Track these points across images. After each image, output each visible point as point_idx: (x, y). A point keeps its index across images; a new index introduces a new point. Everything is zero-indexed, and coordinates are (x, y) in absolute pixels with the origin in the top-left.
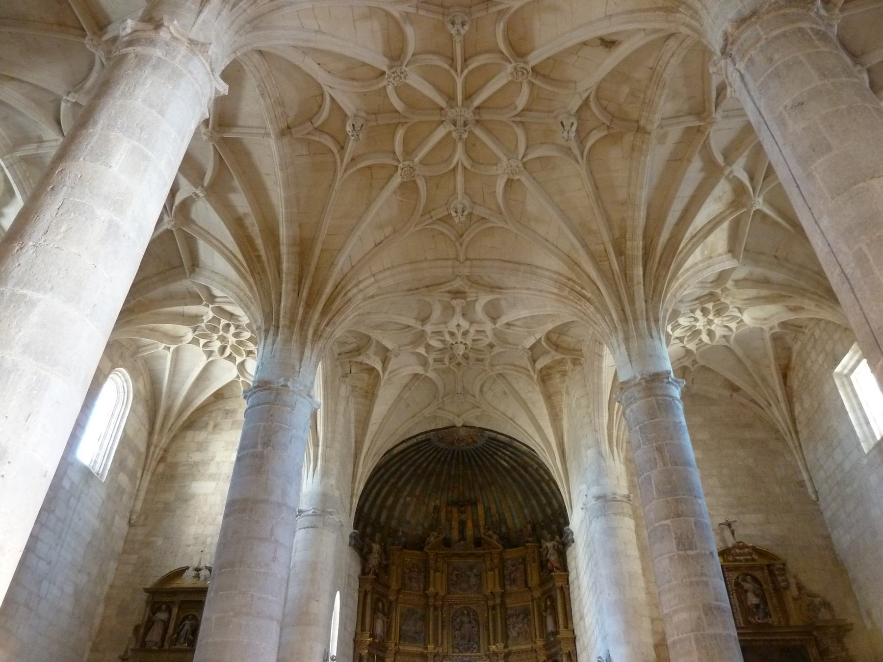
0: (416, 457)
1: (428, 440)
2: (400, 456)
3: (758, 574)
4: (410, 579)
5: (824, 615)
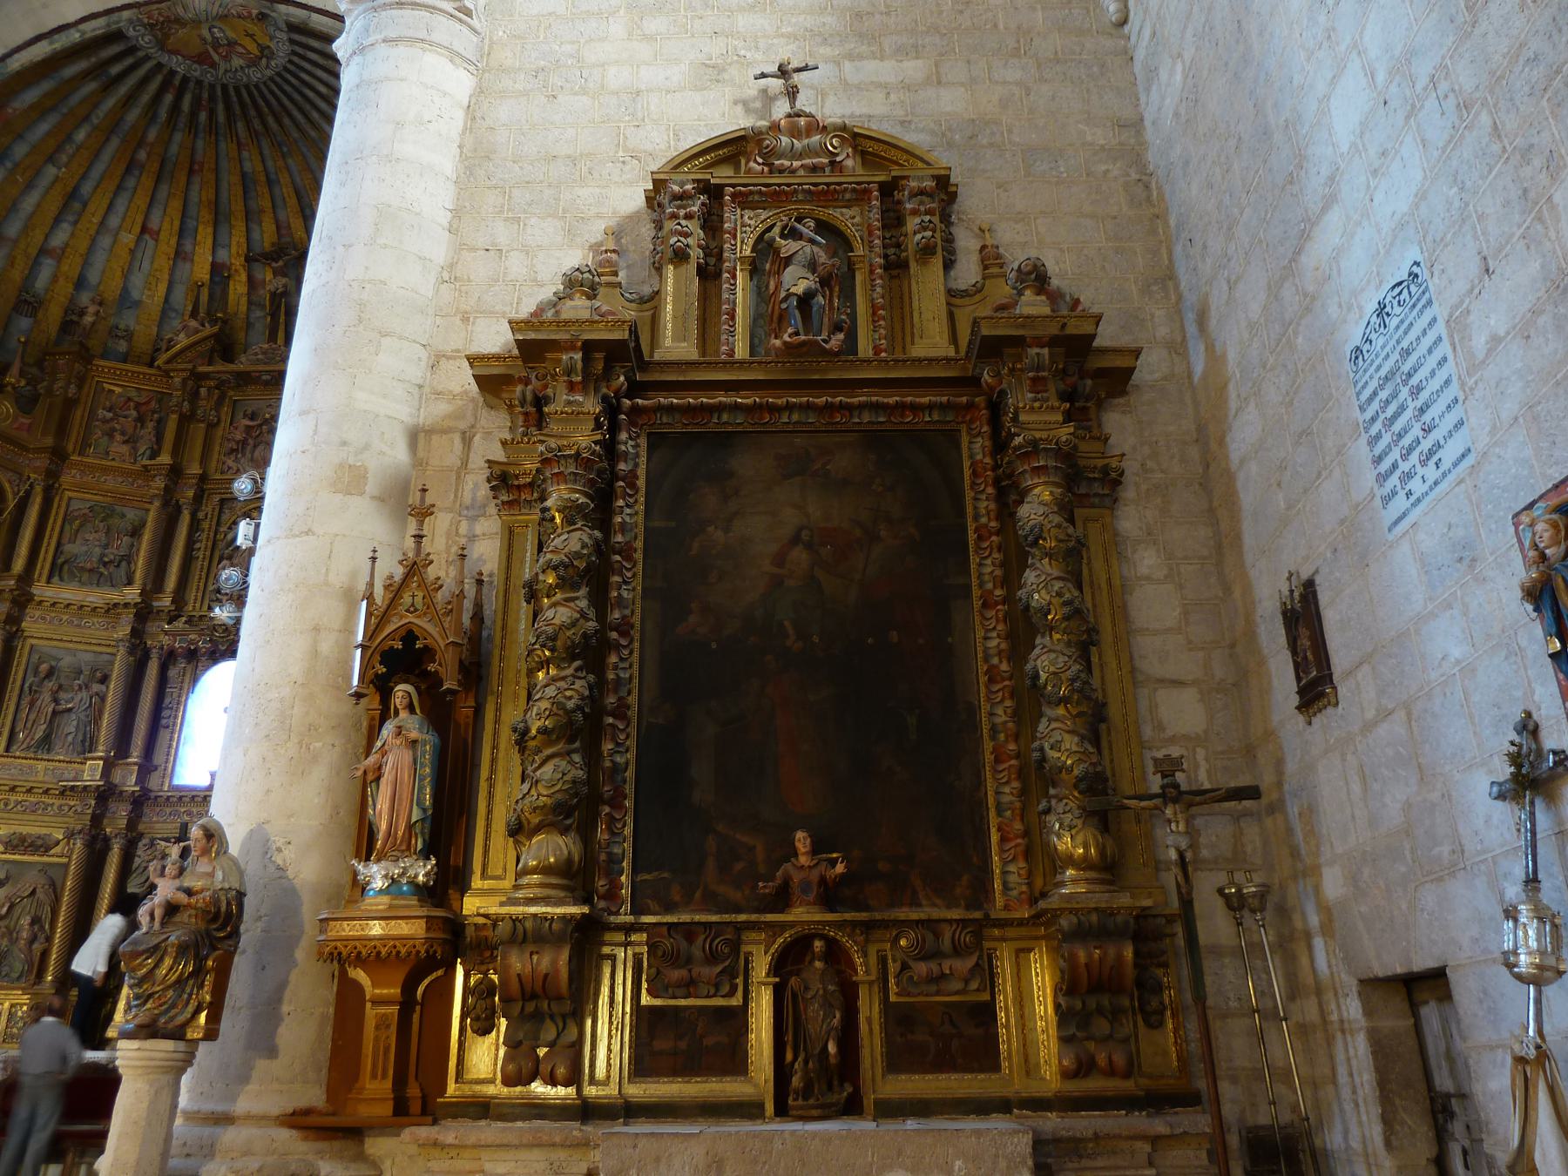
0: (110, 102)
1: (115, 36)
2: (47, 86)
3: (847, 218)
4: (110, 434)
5: (1032, 304)
